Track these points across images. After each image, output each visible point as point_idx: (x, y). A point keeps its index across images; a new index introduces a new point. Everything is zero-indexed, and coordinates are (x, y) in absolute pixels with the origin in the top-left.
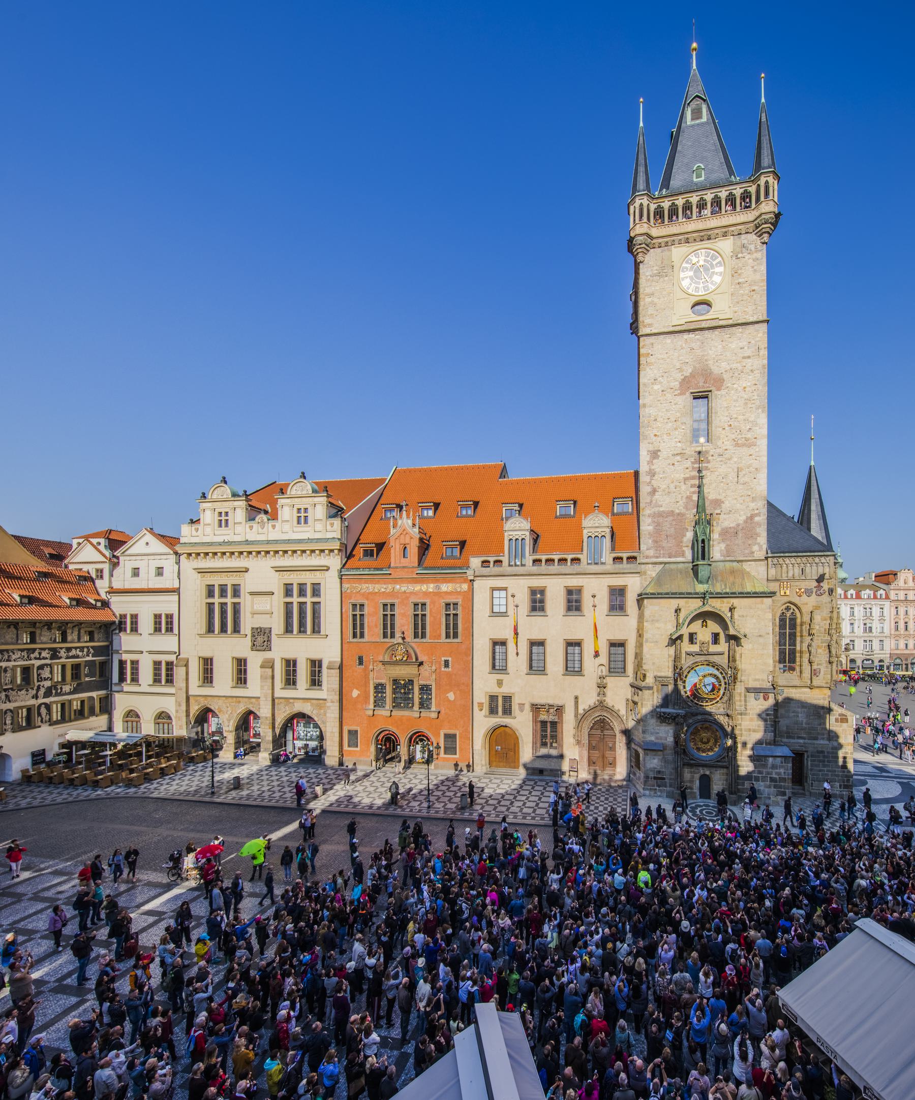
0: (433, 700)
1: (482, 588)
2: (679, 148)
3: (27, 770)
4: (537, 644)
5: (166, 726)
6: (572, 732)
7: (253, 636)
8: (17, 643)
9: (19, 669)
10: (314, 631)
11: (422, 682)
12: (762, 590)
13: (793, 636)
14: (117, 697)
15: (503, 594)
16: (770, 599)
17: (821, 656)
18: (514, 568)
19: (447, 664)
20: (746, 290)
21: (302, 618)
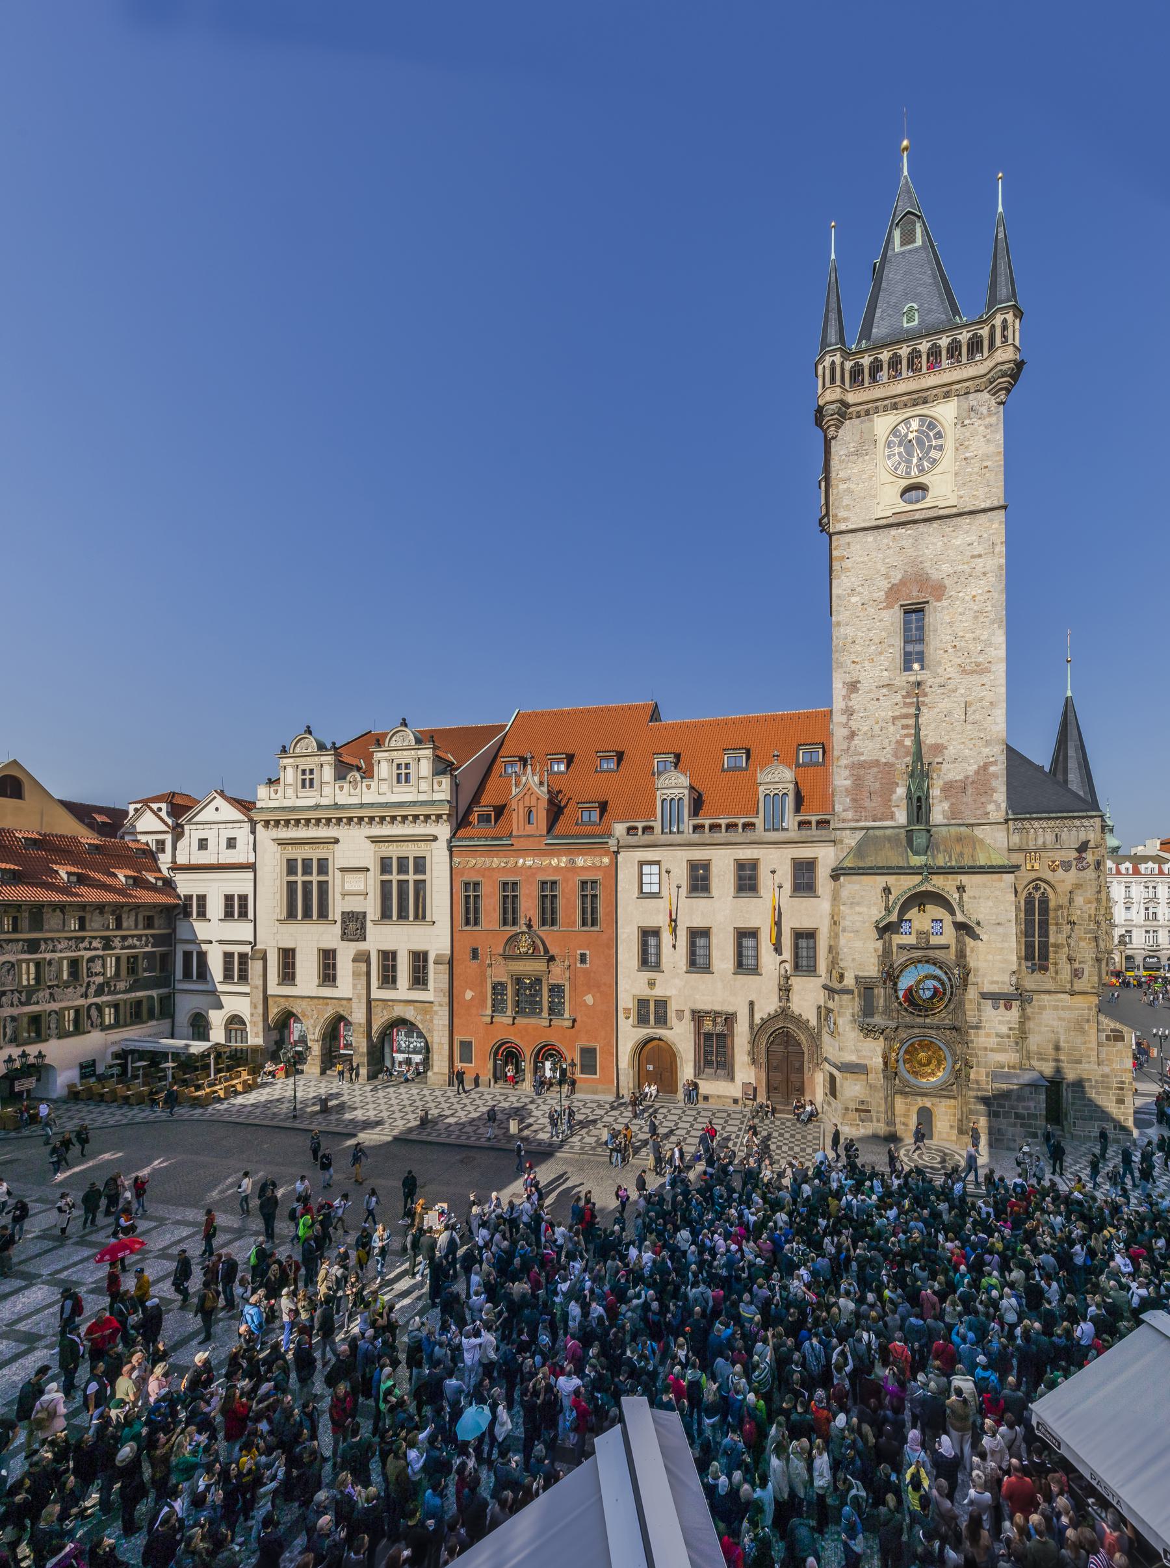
0: (567, 1004)
1: (628, 861)
2: (884, 285)
3: (74, 1085)
4: (699, 935)
5: (239, 1033)
7: (343, 922)
8: (63, 931)
9: (65, 962)
10: (416, 917)
11: (551, 982)
13: (1044, 925)
15: (655, 869)
16: (1012, 876)
17: (1085, 951)
19: (583, 958)
20: (975, 467)
21: (402, 900)
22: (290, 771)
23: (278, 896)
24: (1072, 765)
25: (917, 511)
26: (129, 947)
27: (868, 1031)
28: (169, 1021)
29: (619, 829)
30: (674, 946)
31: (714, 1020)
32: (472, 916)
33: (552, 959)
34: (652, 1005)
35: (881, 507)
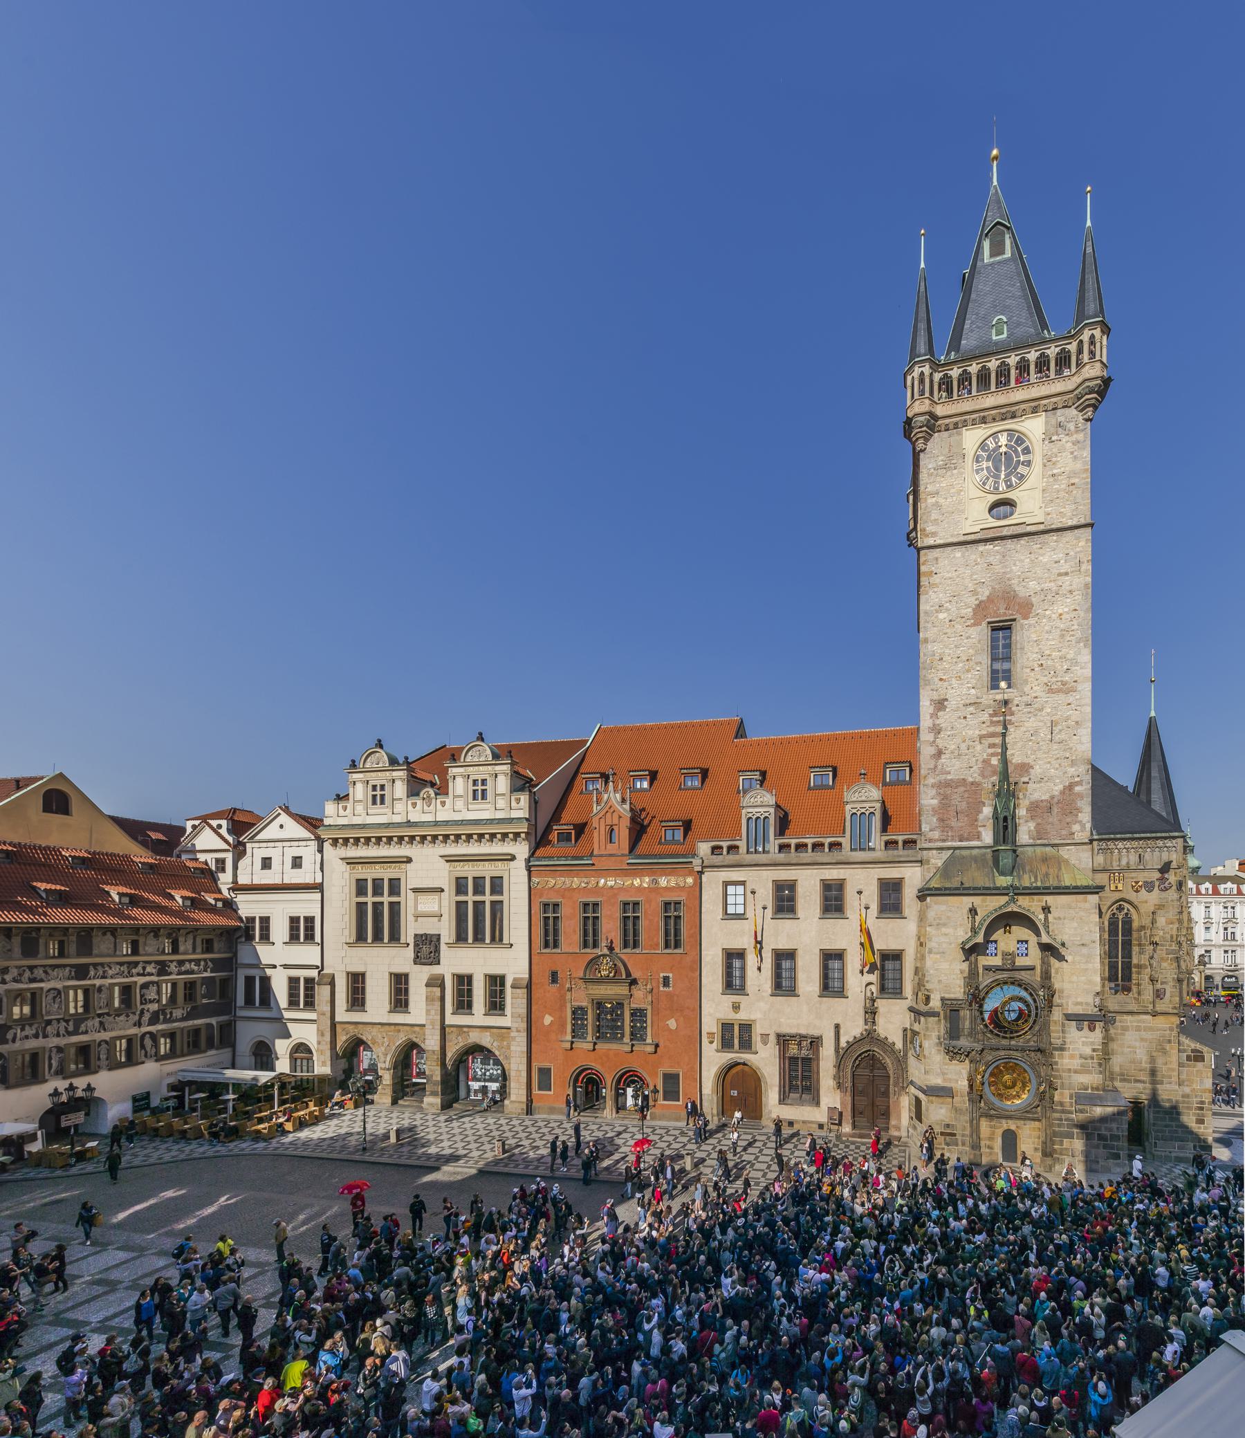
0: (649, 1029)
1: (713, 882)
2: (973, 296)
4: (785, 958)
5: (305, 1062)
6: (832, 1071)
7: (416, 945)
8: (115, 955)
9: (117, 989)
10: (493, 939)
11: (633, 1006)
12: (1085, 883)
13: (1127, 945)
14: (240, 1026)
15: (740, 889)
16: (1096, 897)
17: (1168, 972)
18: (754, 856)
19: (666, 982)
21: (478, 921)
22: (359, 786)
23: (347, 918)
24: (1156, 786)
25: (1004, 528)
26: (187, 972)
27: (953, 1054)
28: (229, 1049)
29: (704, 848)
30: (759, 969)
31: (799, 1044)
32: (551, 938)
33: (634, 982)
34: (736, 1028)
35: (969, 522)
